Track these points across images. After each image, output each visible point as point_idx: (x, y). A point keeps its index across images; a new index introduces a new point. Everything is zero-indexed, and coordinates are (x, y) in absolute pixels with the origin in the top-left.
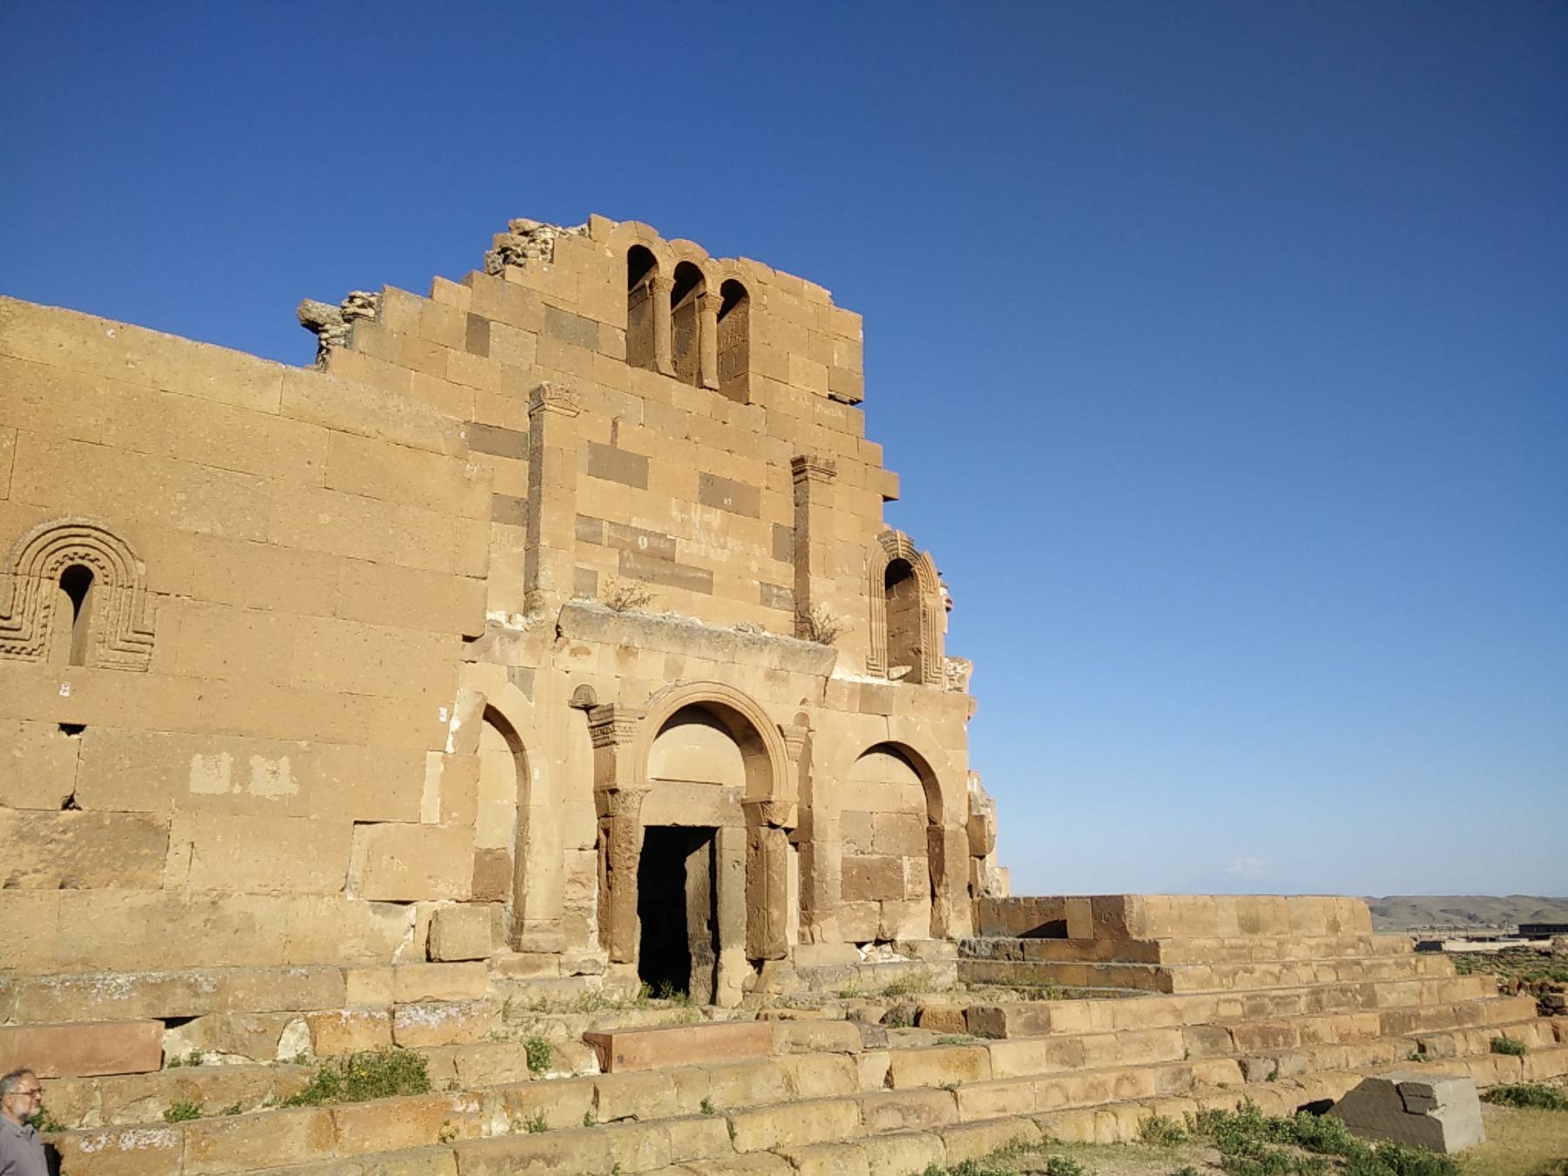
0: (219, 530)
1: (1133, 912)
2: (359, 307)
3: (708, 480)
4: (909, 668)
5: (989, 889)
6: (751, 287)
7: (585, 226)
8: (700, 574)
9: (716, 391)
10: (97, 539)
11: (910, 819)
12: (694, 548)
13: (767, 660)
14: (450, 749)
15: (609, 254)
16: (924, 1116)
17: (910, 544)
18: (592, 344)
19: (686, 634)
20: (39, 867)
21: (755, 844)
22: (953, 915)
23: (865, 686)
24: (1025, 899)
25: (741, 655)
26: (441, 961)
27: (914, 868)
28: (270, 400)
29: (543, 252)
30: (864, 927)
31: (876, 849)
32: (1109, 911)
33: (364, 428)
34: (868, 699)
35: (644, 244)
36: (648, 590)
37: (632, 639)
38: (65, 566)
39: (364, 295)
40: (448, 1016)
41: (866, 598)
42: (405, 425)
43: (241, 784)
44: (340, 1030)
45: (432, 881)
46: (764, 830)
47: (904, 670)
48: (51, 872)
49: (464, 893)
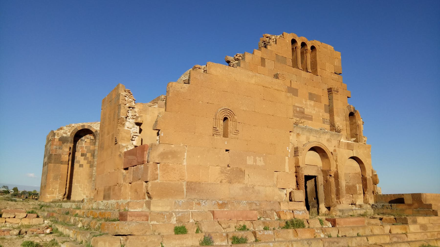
0: (247, 109)
1: (423, 197)
2: (238, 57)
3: (310, 94)
4: (355, 139)
5: (378, 192)
6: (317, 47)
7: (281, 35)
8: (310, 117)
9: (311, 73)
10: (229, 112)
11: (358, 175)
12: (308, 110)
13: (327, 136)
14: (289, 156)
15: (287, 41)
16: (401, 239)
17: (354, 108)
18: (285, 63)
19: (310, 131)
20: (225, 178)
21: (326, 180)
22: (370, 198)
23: (348, 143)
24: (389, 195)
25: (322, 136)
26: (295, 201)
27: (359, 187)
28: (253, 81)
29: (273, 42)
30: (349, 200)
31: (351, 182)
32: (417, 197)
33: (269, 86)
34: (349, 146)
35: (294, 38)
36: (303, 120)
37: (299, 132)
38: (224, 117)
39: (240, 54)
40: (303, 213)
41: (345, 122)
42: (276, 85)
43: (255, 163)
44: (284, 214)
45: (288, 185)
46: (328, 177)
47: (354, 139)
48: (227, 180)
49: (294, 187)
